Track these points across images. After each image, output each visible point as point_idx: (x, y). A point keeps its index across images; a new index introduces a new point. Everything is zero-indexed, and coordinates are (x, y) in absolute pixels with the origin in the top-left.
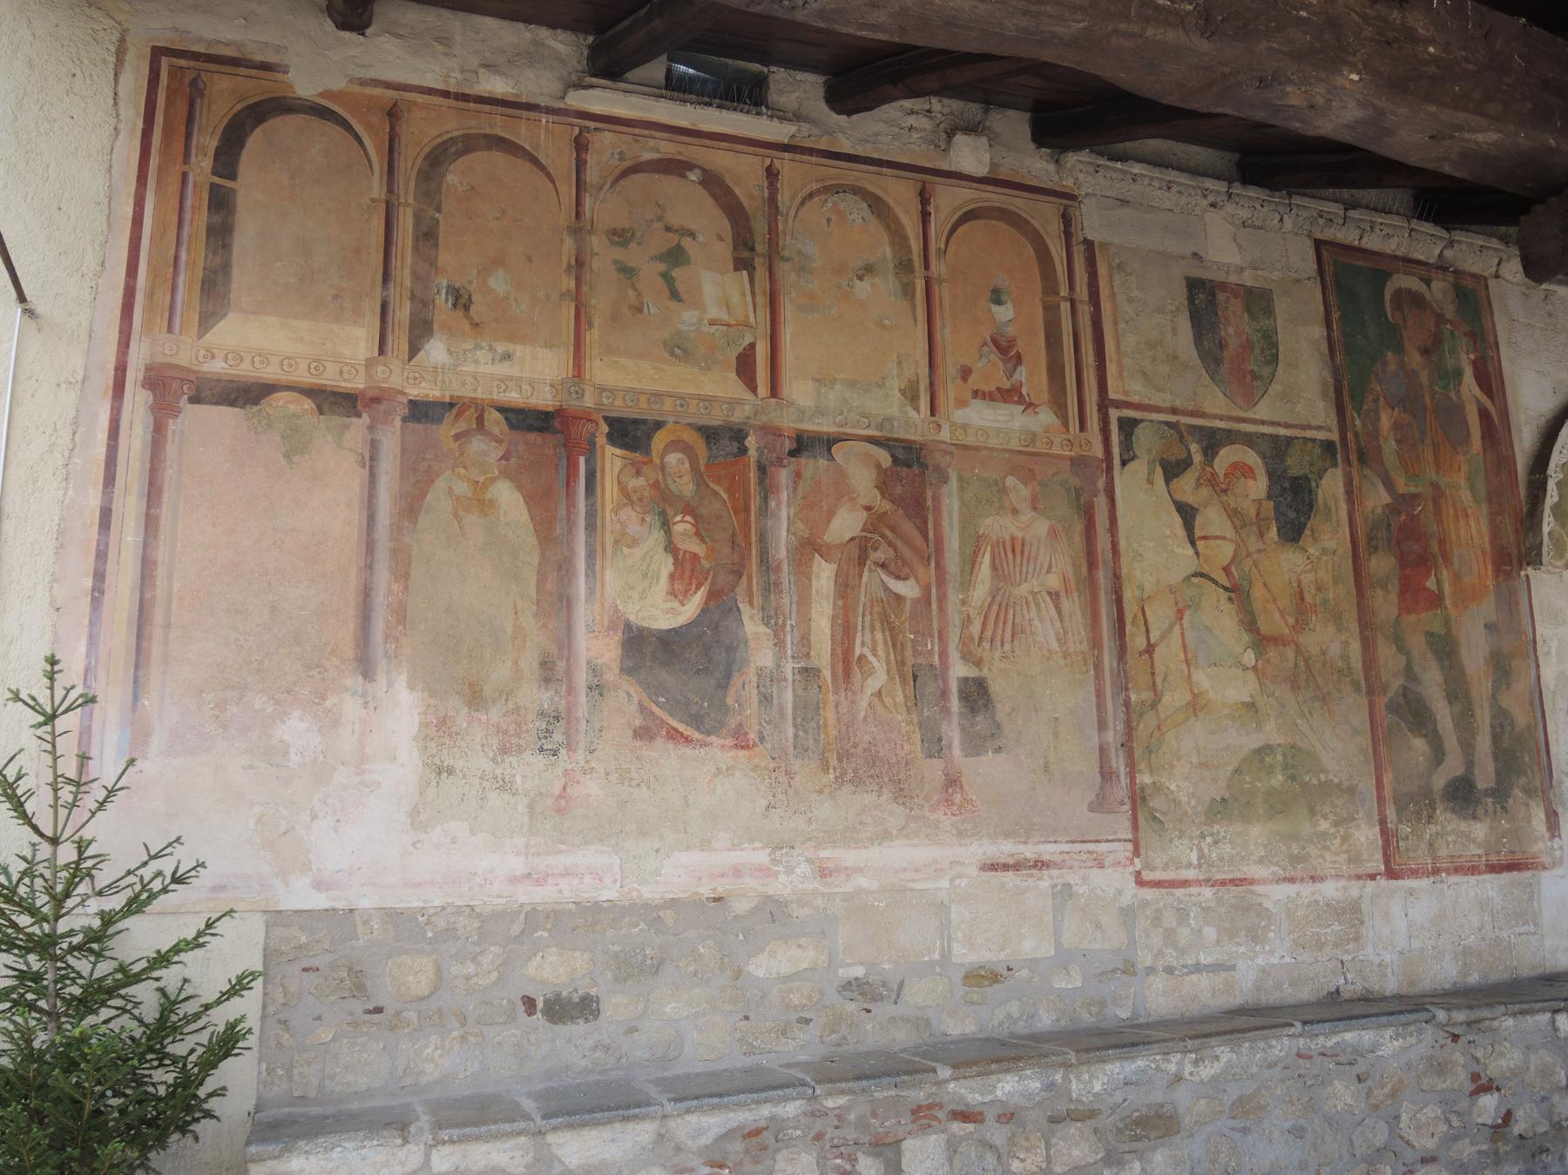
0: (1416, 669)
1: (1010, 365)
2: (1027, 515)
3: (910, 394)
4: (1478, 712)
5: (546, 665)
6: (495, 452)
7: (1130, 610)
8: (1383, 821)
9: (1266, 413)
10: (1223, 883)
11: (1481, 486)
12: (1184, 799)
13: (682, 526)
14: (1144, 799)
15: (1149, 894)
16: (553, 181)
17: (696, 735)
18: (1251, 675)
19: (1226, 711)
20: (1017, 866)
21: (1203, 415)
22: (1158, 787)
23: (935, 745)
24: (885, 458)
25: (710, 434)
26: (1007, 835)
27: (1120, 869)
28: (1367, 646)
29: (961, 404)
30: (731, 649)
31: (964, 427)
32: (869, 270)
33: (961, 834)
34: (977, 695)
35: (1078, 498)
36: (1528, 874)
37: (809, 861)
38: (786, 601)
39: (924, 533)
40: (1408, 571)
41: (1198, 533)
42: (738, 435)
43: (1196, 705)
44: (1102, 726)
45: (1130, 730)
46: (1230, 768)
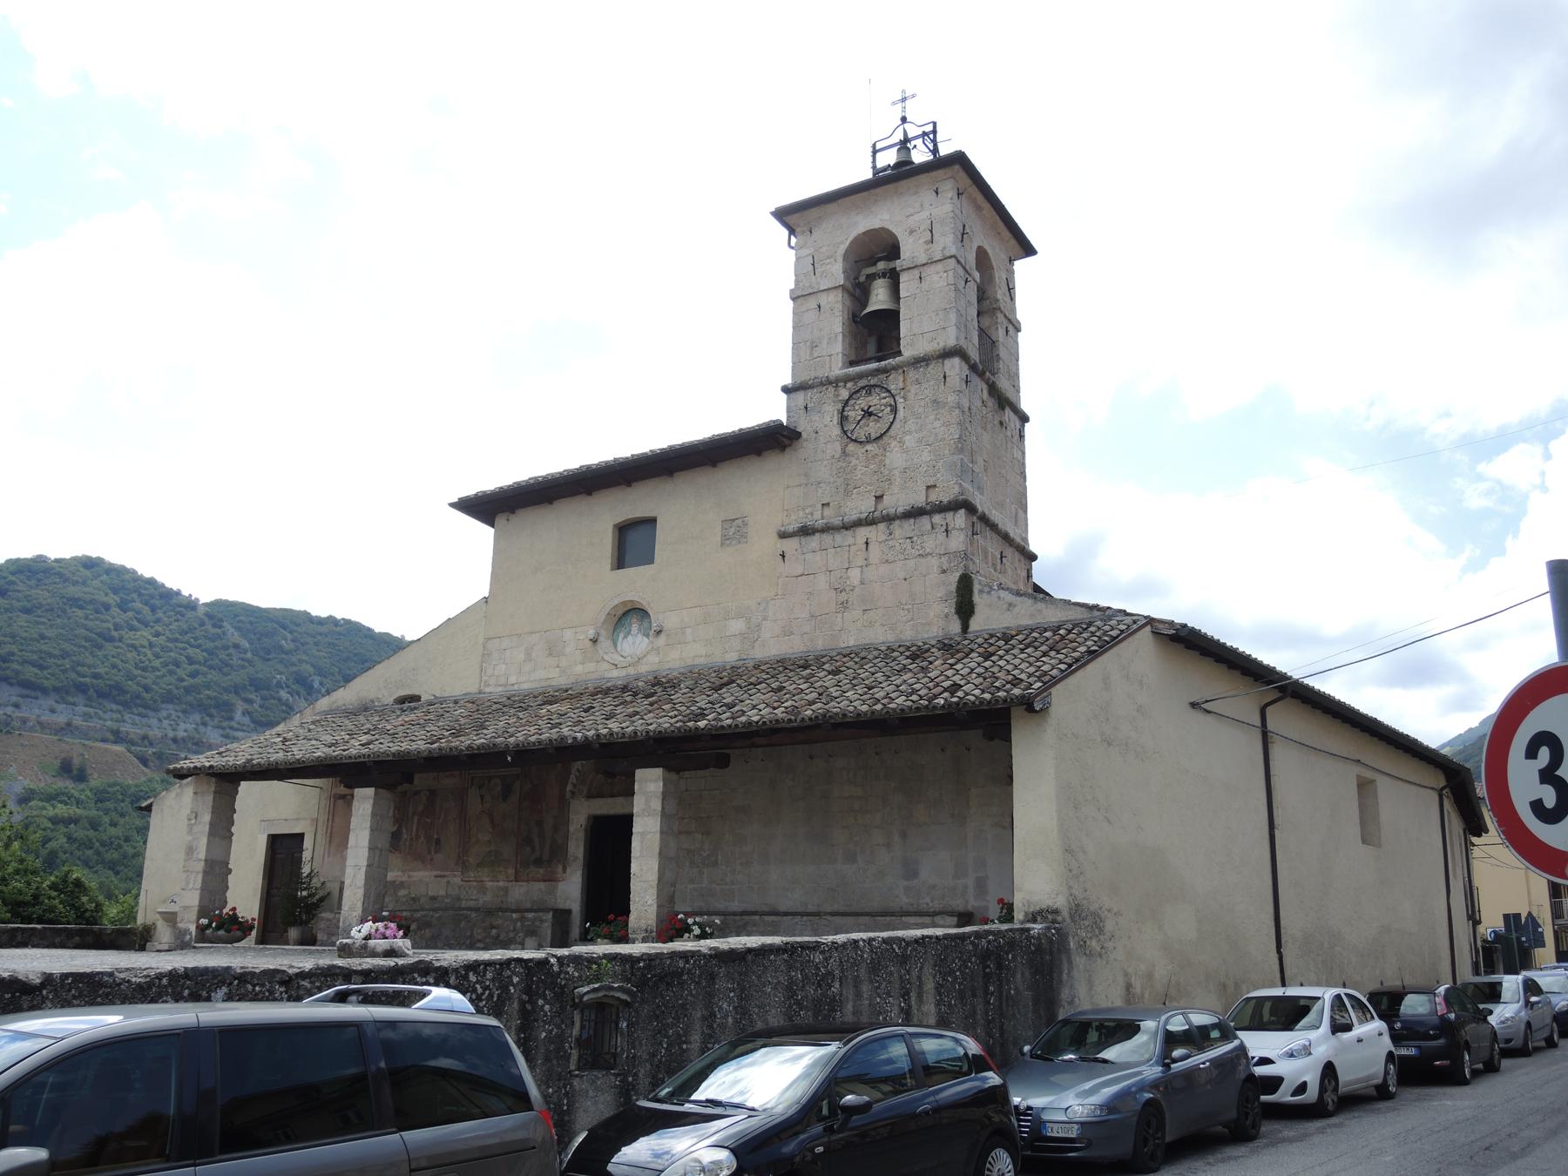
34: (438, 842)
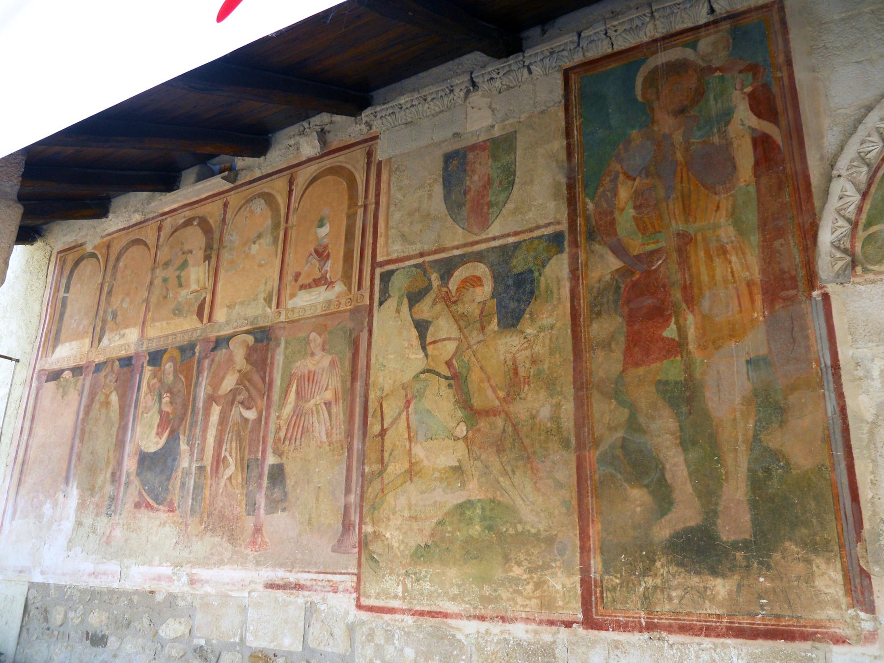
0: (642, 420)
1: (322, 263)
2: (319, 354)
3: (268, 300)
4: (729, 458)
5: (113, 474)
6: (112, 378)
7: (372, 406)
8: (585, 571)
9: (500, 229)
10: (422, 614)
11: (751, 217)
12: (396, 545)
13: (166, 399)
14: (366, 544)
15: (364, 615)
16: (149, 249)
17: (155, 505)
18: (461, 445)
19: (437, 475)
20: (284, 587)
21: (444, 250)
22: (377, 535)
23: (252, 507)
24: (250, 339)
25: (182, 349)
26: (281, 565)
27: (347, 595)
28: (582, 404)
29: (293, 296)
30: (174, 460)
31: (293, 310)
32: (260, 236)
33: (258, 564)
34: (278, 475)
35: (350, 336)
36: (807, 645)
37: (187, 574)
38: (198, 431)
39: (264, 381)
40: (637, 327)
41: (429, 340)
42: (192, 346)
43: (412, 472)
44: (348, 491)
45: (363, 493)
46: (435, 521)
